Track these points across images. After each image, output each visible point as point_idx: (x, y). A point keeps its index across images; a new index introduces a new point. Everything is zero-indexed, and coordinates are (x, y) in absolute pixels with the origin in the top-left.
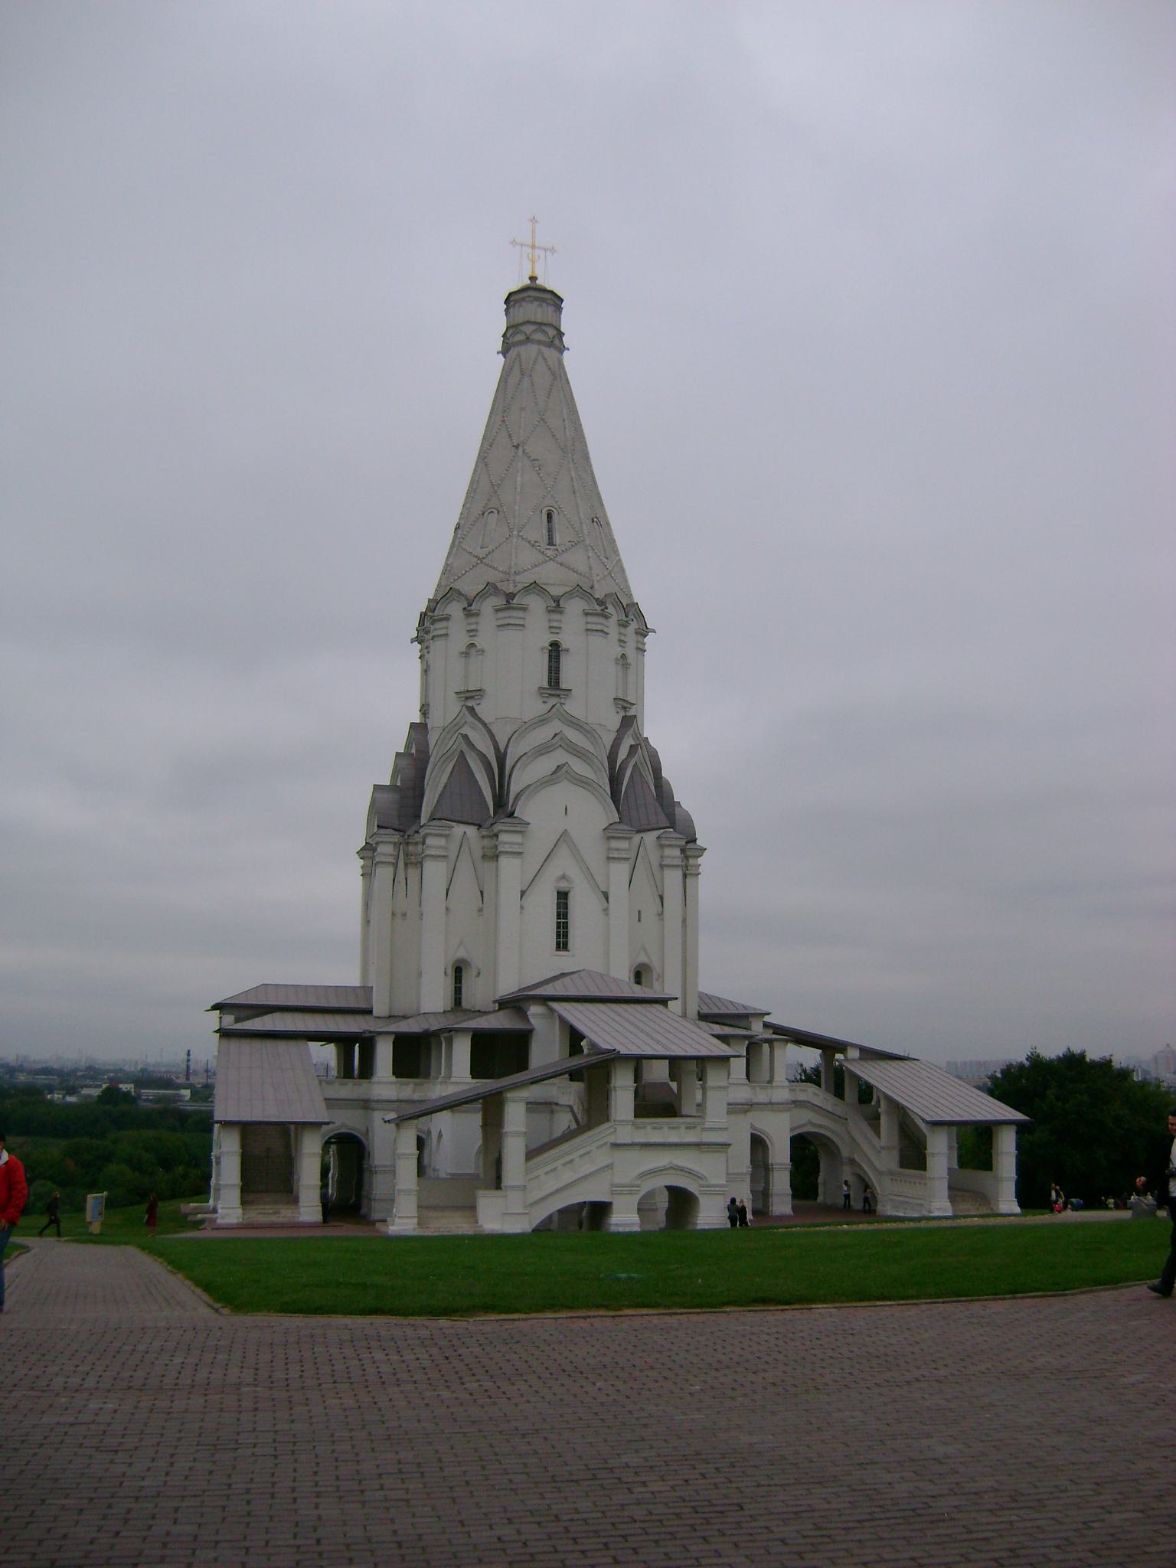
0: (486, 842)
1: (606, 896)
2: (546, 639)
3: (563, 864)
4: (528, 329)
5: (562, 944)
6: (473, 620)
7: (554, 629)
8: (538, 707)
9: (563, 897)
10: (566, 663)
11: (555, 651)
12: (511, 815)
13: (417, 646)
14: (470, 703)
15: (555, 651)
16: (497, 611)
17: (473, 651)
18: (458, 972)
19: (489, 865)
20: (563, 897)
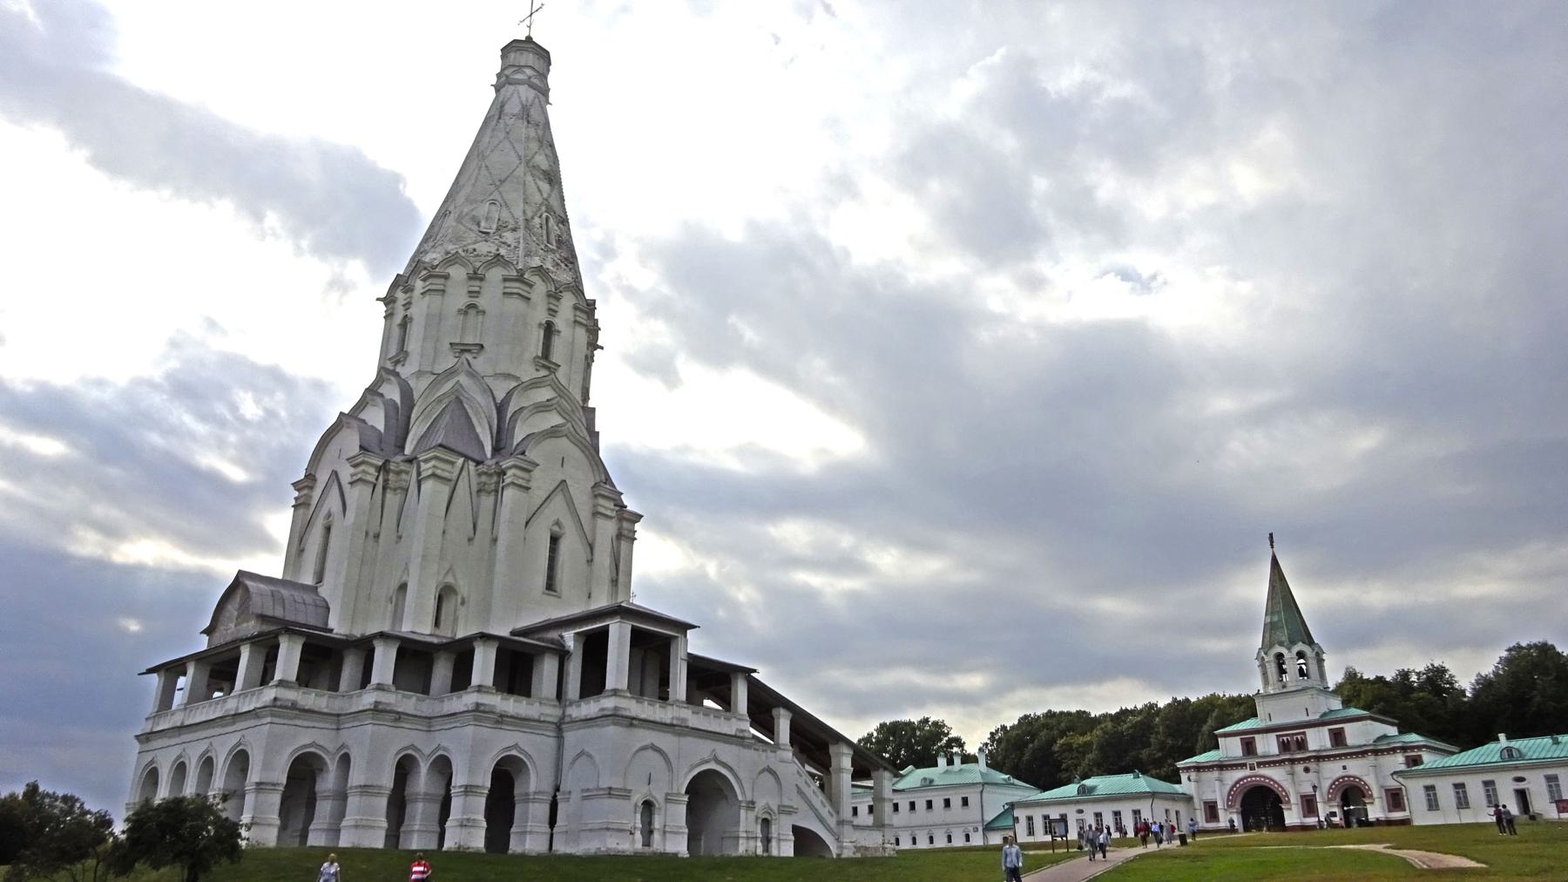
0: (484, 479)
1: (591, 547)
2: (542, 316)
3: (557, 508)
4: (529, 72)
5: (550, 585)
6: (477, 283)
7: (552, 312)
8: (528, 373)
9: (555, 540)
10: (558, 345)
11: (549, 330)
12: (523, 453)
13: (382, 307)
14: (468, 356)
15: (549, 330)
16: (505, 280)
17: (472, 312)
18: (440, 600)
19: (487, 501)
20: (555, 540)
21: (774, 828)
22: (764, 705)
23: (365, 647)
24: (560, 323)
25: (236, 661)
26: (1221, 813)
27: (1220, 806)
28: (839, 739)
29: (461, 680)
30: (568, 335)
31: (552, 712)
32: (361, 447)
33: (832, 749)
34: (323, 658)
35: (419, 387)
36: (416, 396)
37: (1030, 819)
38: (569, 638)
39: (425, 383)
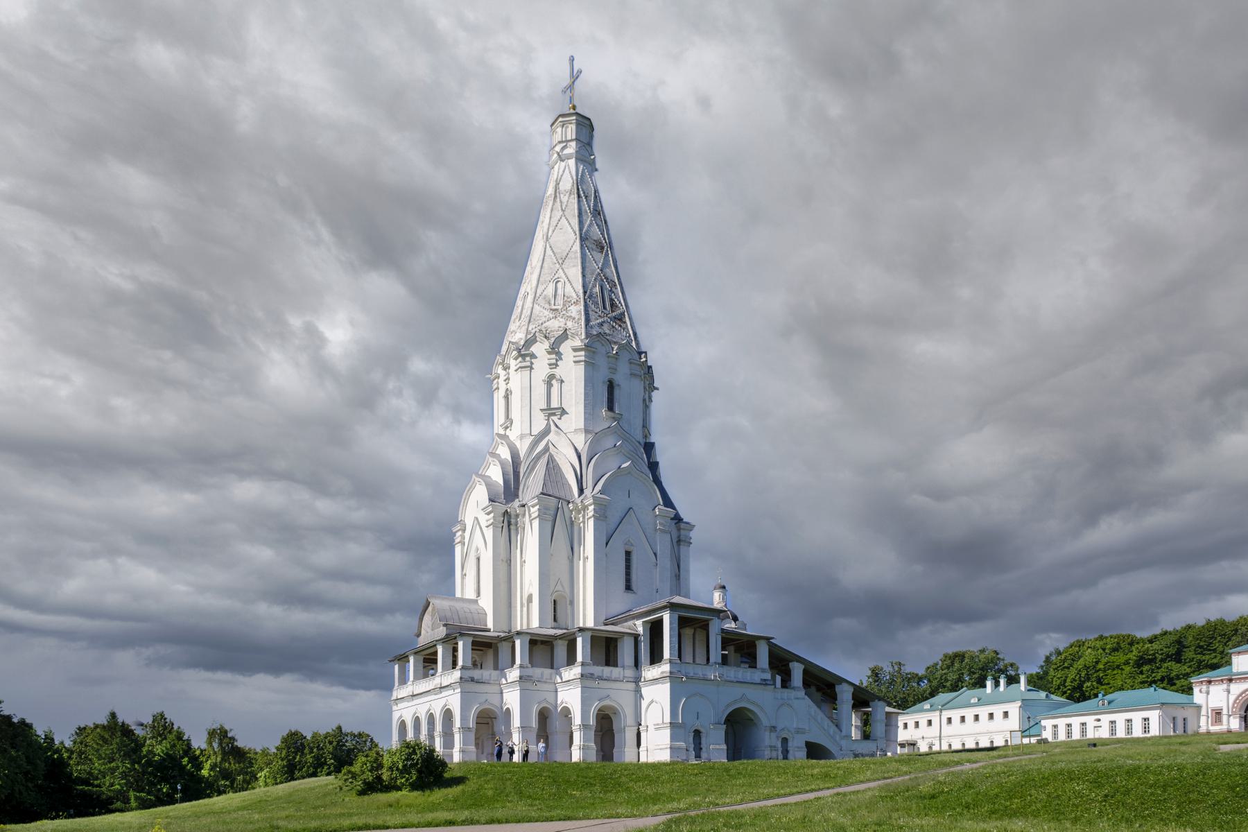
14: (555, 418)
20: (628, 554)
21: (790, 744)
22: (781, 662)
23: (509, 639)
24: (619, 379)
25: (436, 653)
26: (1225, 718)
27: (1225, 712)
28: (842, 680)
29: (571, 660)
30: (629, 388)
31: (630, 673)
32: (491, 500)
33: (838, 688)
34: (487, 649)
35: (523, 447)
36: (522, 456)
37: (1069, 725)
38: (639, 626)
39: (528, 441)
